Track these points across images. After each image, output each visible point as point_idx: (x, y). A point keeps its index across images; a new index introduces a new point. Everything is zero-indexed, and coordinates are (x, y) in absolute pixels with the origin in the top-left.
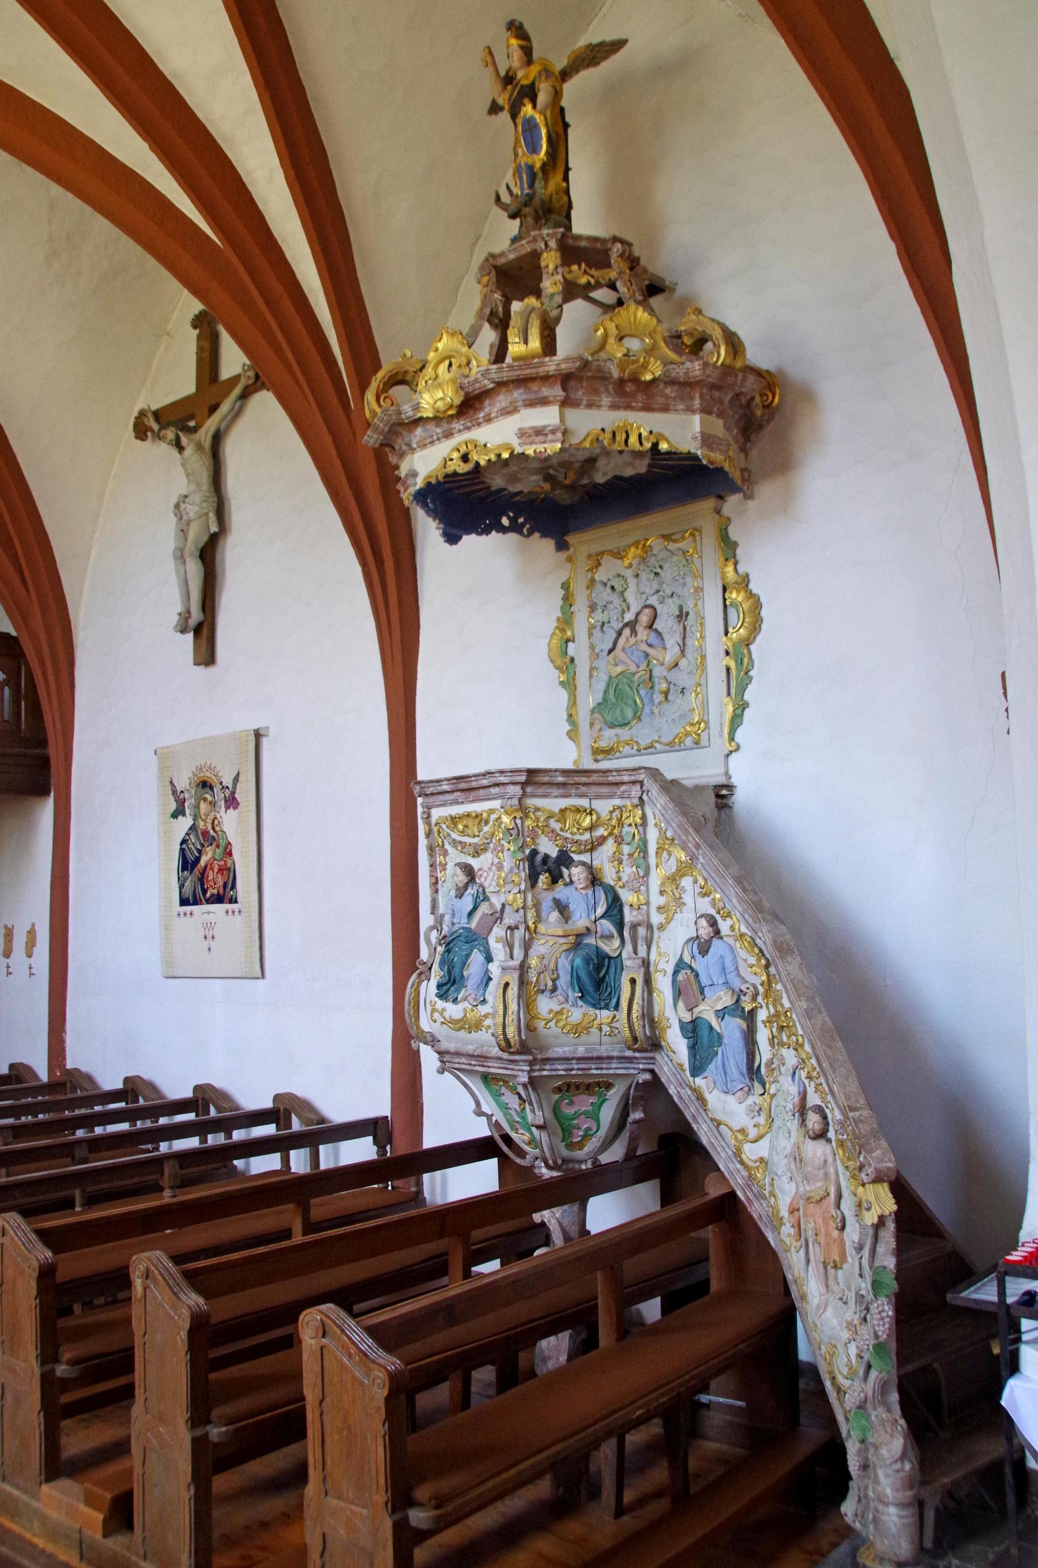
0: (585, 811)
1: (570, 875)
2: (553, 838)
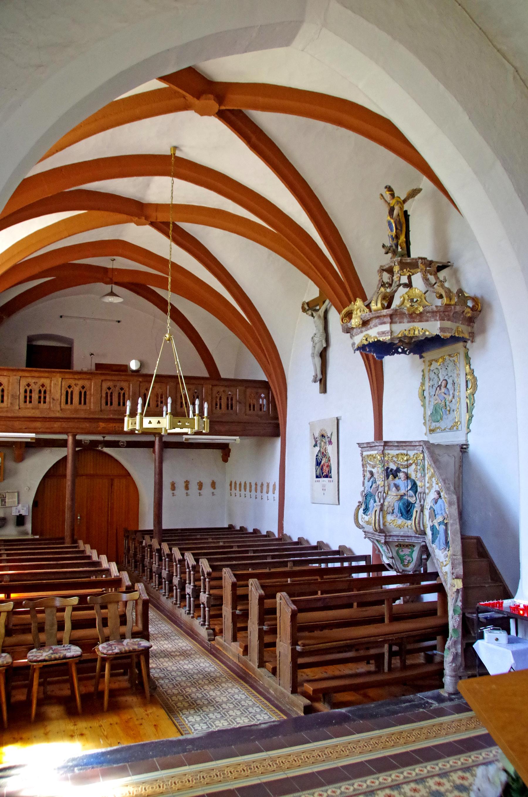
0: (405, 455)
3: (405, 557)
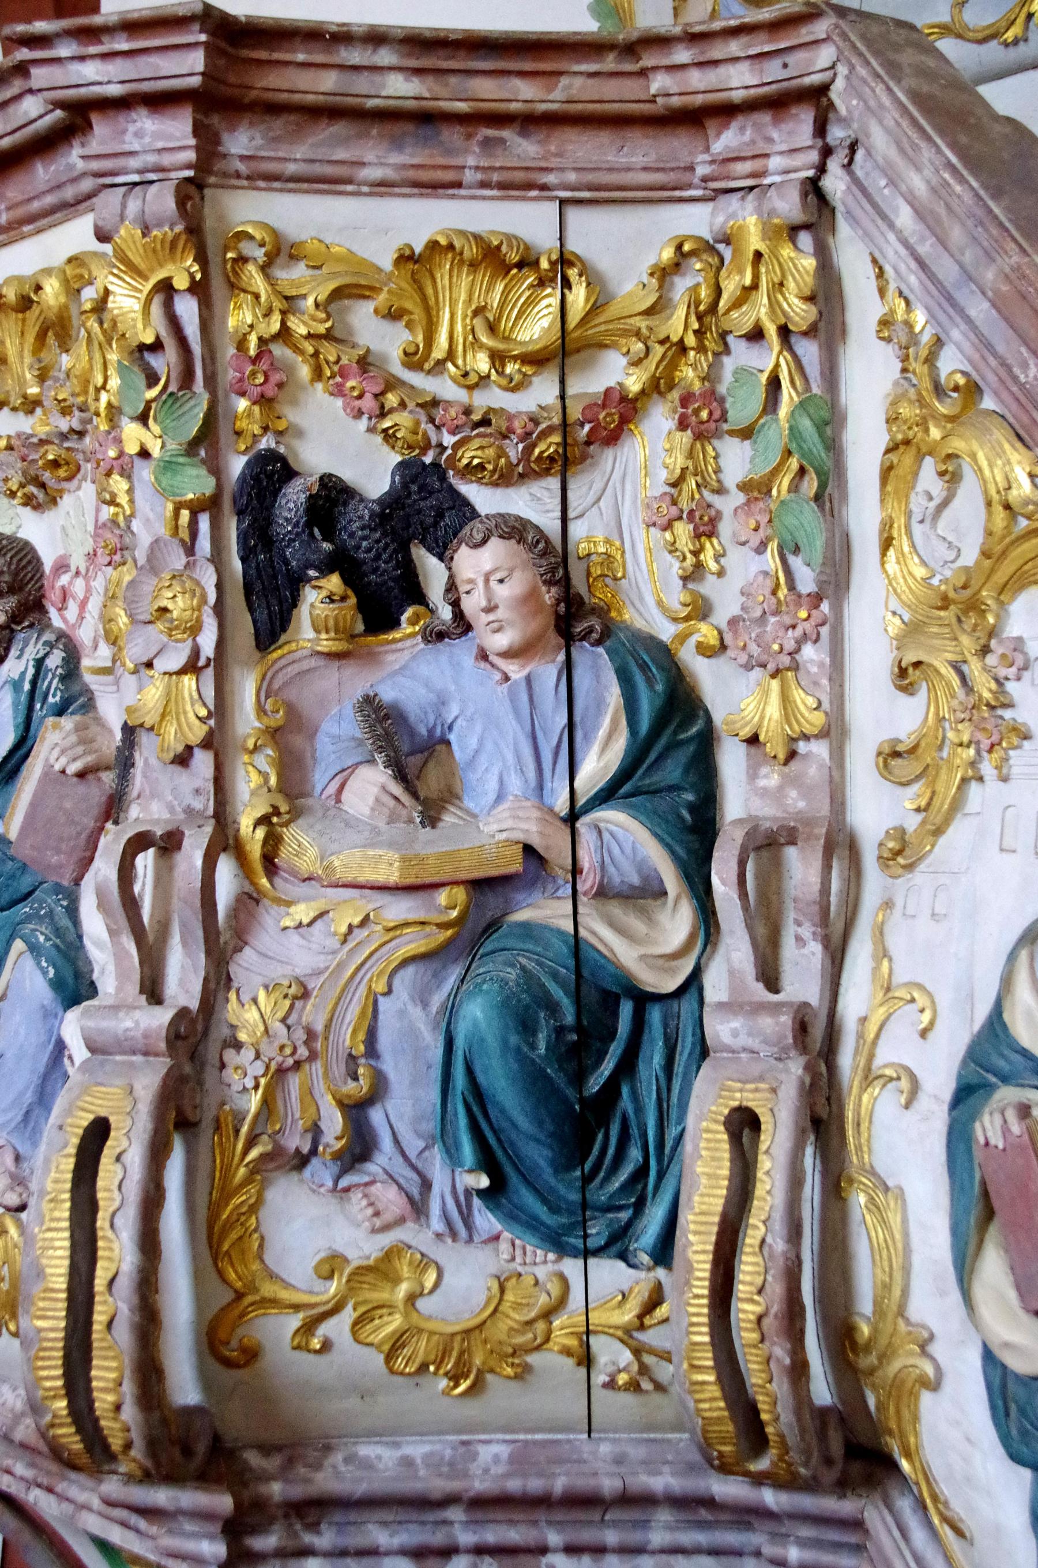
0: (527, 262)
1: (451, 586)
2: (368, 403)
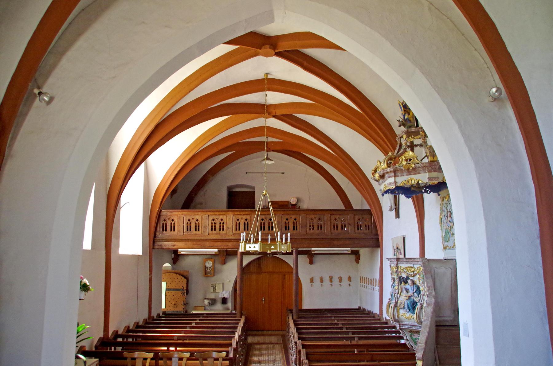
3: (416, 340)
